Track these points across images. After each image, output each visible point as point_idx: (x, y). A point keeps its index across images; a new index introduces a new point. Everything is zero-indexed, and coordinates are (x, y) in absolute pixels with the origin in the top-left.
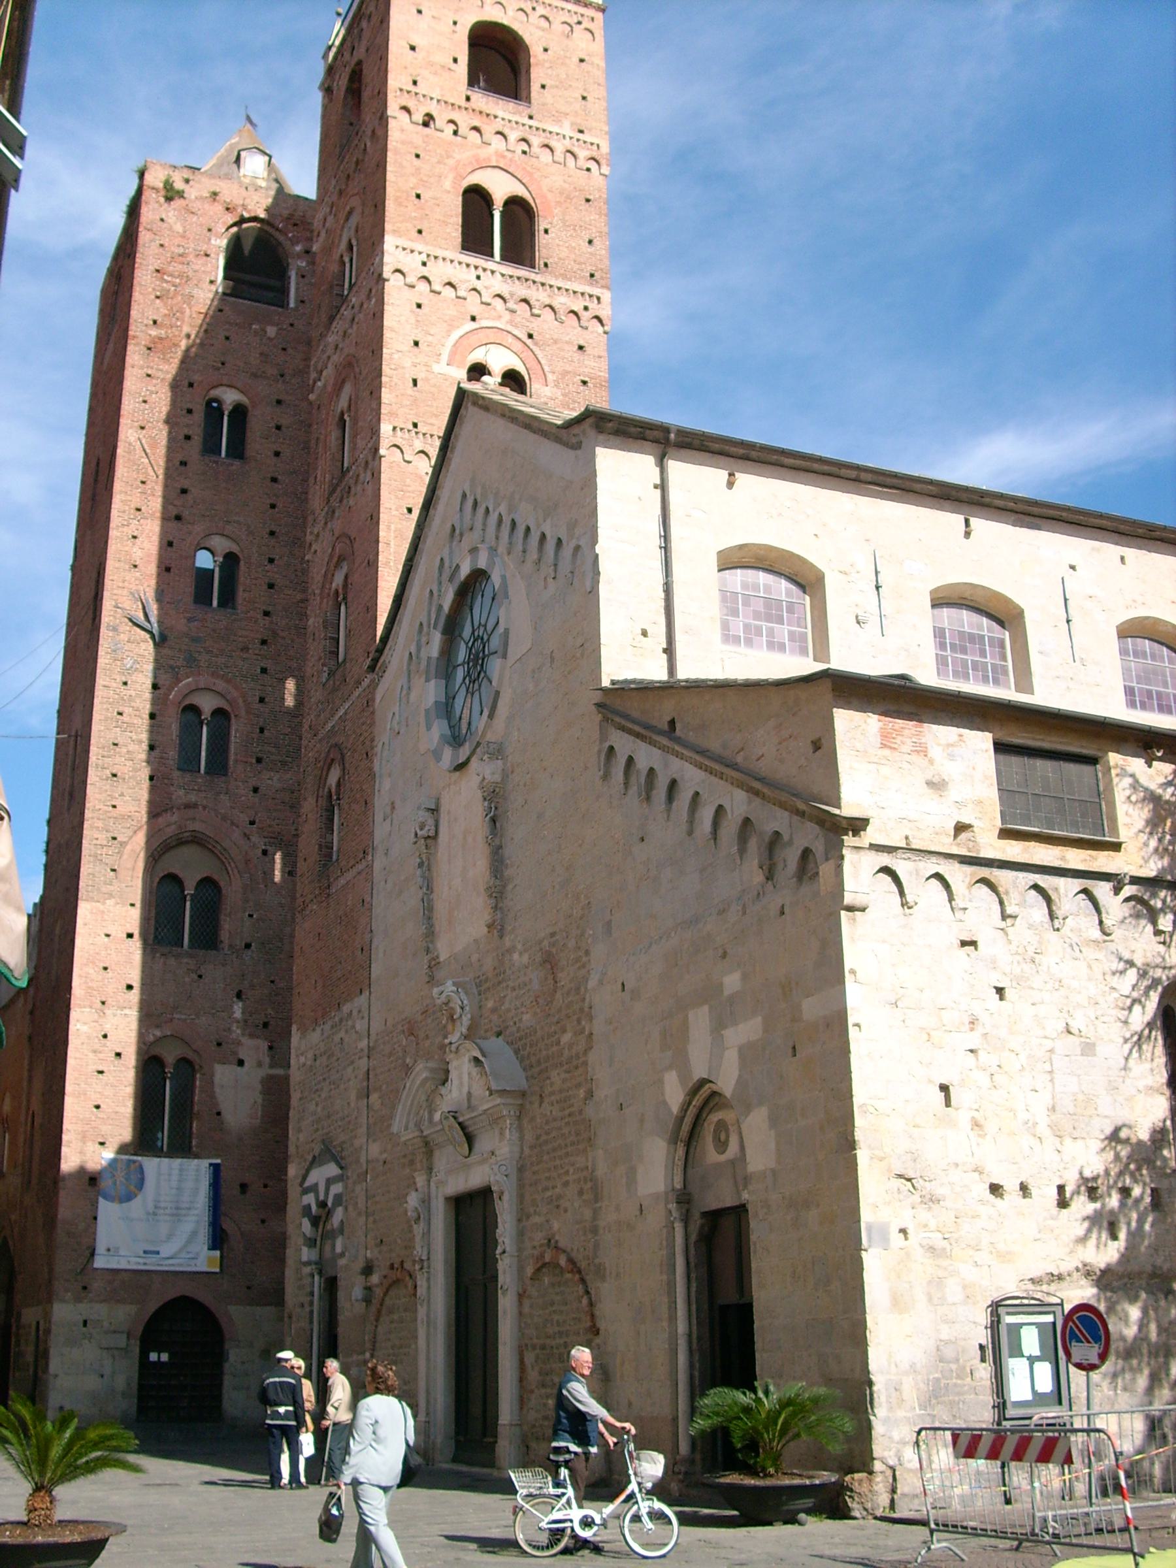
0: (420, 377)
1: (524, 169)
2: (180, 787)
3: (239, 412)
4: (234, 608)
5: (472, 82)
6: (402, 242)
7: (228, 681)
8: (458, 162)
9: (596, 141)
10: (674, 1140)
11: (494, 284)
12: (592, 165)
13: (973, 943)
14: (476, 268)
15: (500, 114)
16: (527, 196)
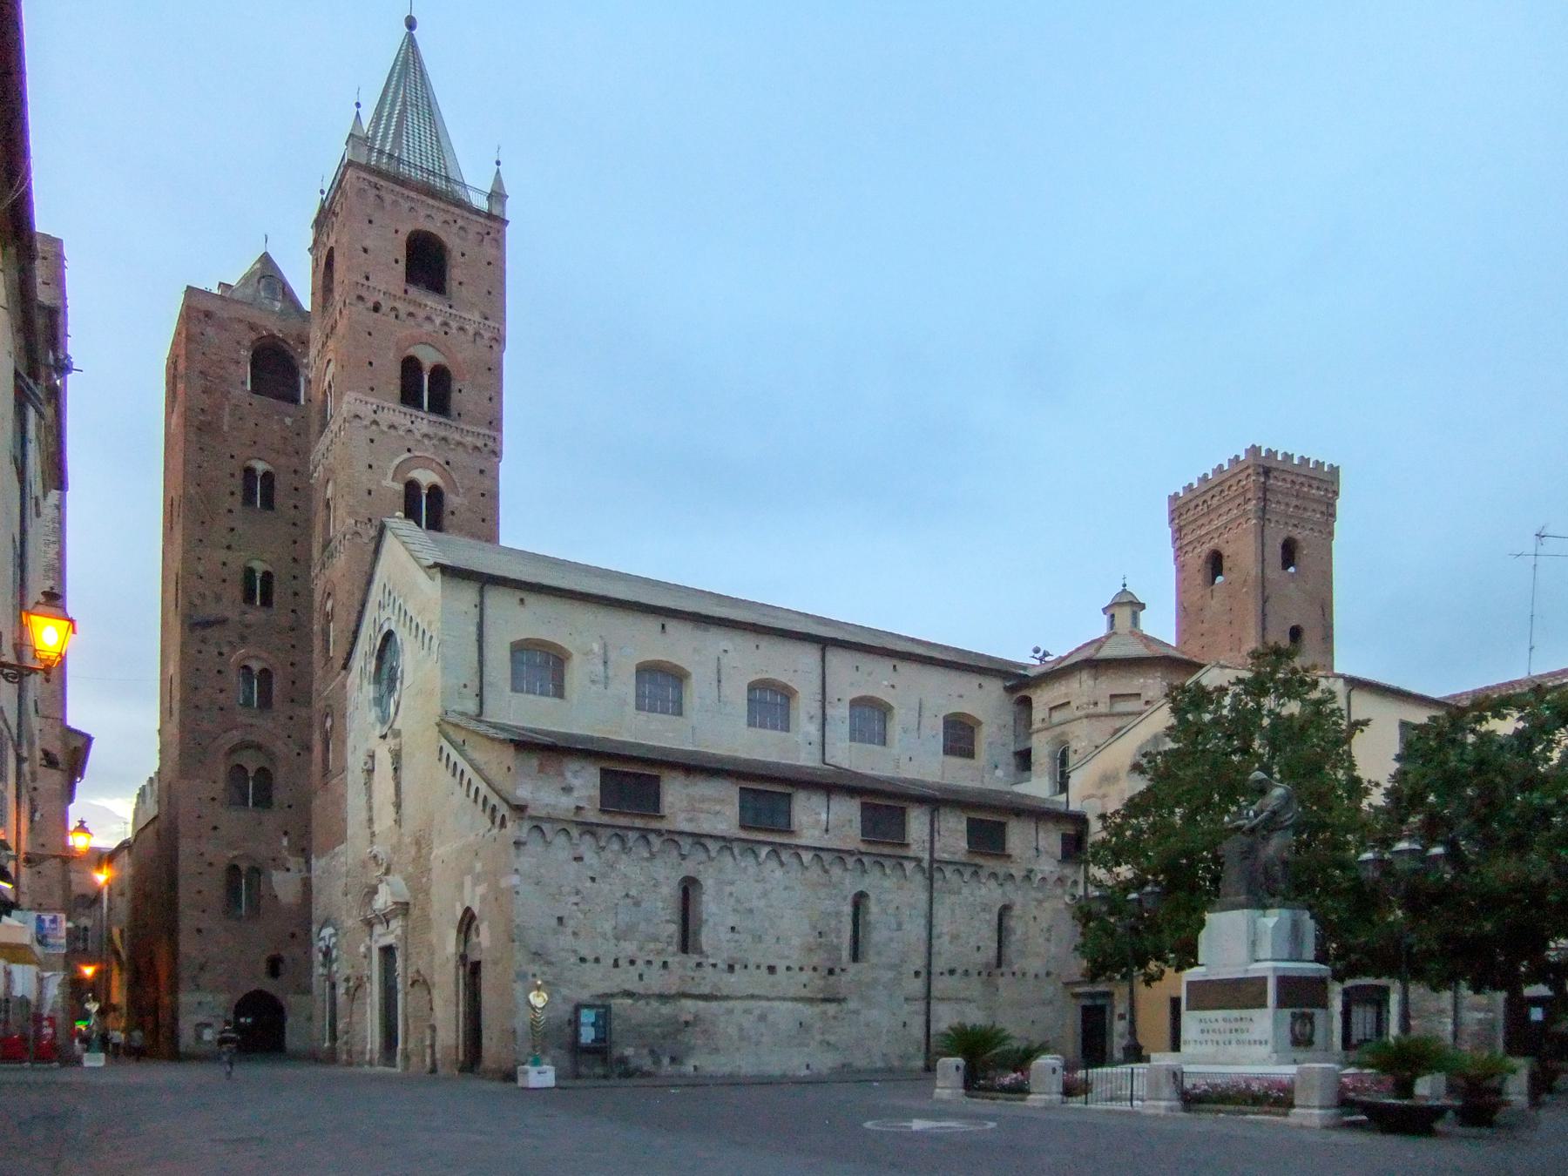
0: (374, 487)
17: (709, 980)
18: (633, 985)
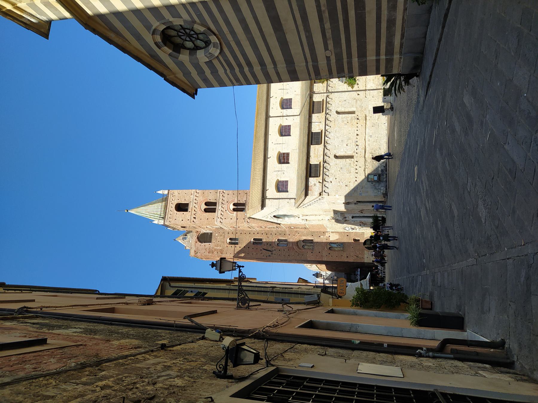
3: (230, 239)
5: (186, 210)
11: (220, 207)
17: (361, 151)
18: (363, 168)
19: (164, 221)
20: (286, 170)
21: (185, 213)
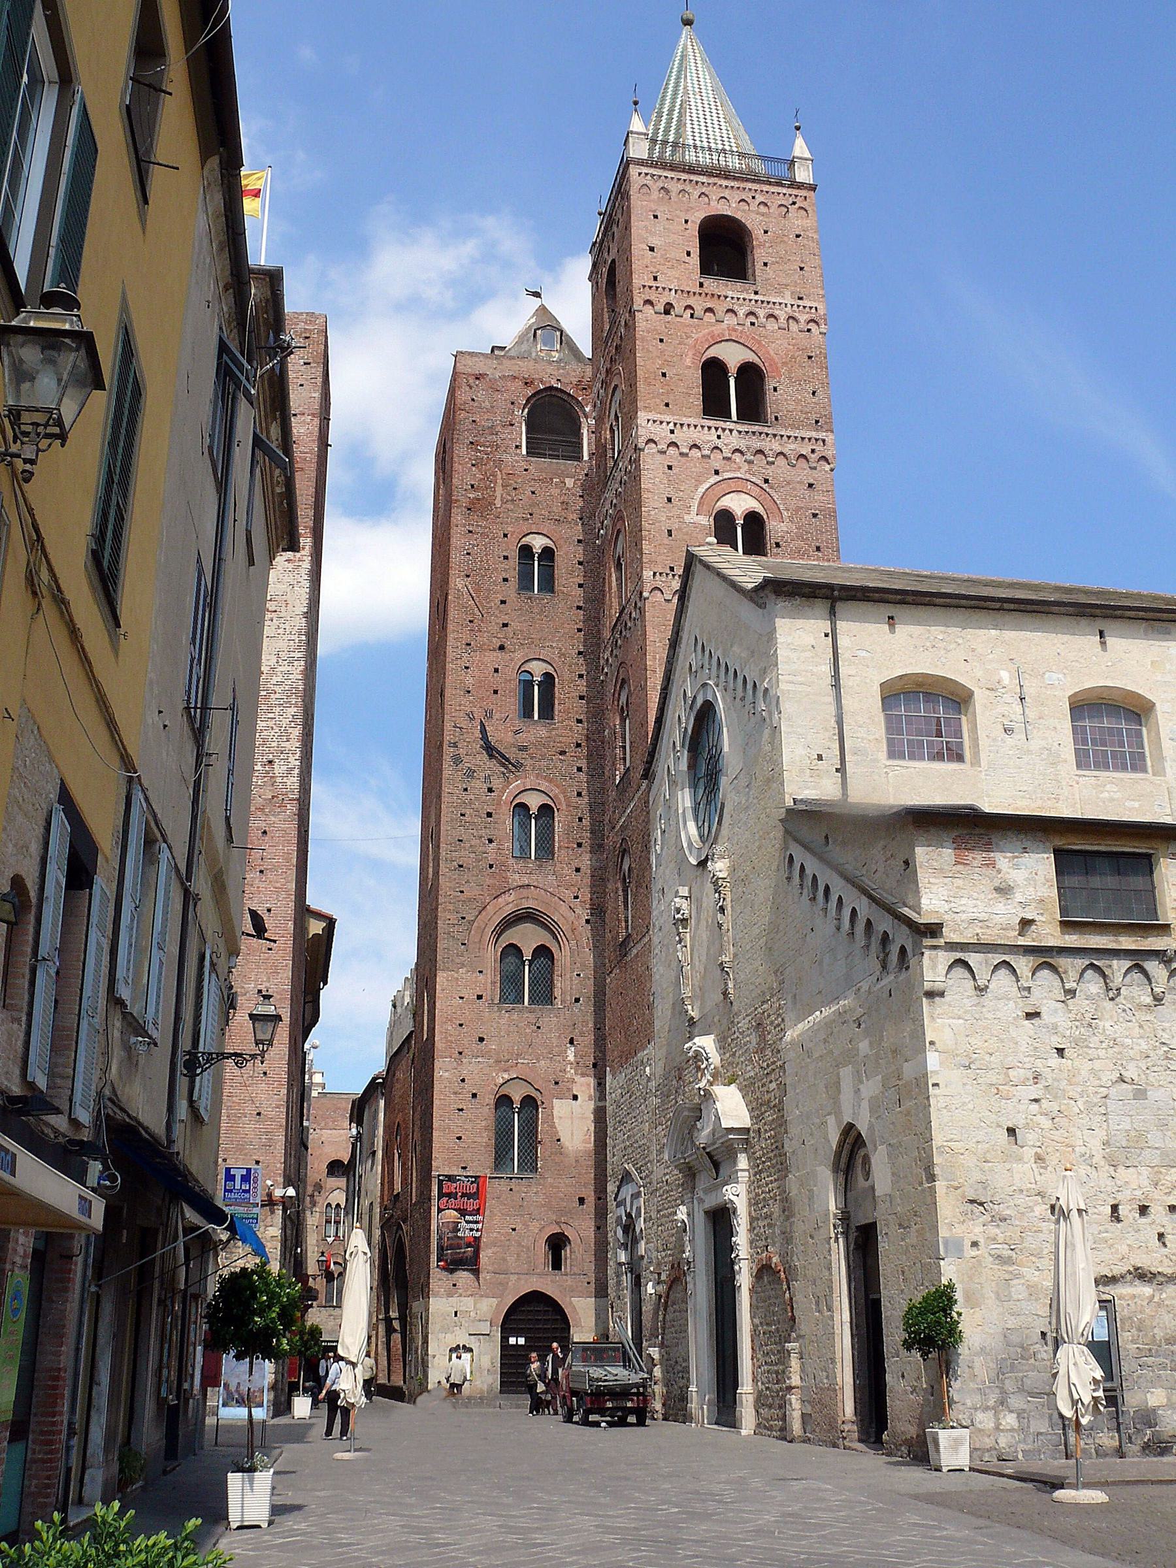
0: (674, 527)
1: (753, 338)
2: (514, 872)
4: (553, 719)
5: (706, 269)
6: (651, 416)
7: (550, 781)
8: (697, 340)
9: (814, 305)
10: (836, 1169)
11: (734, 441)
12: (812, 326)
13: (1037, 1014)
14: (717, 429)
15: (730, 294)
16: (757, 360)
19: (641, 163)
20: (1035, 744)
21: (695, 259)
